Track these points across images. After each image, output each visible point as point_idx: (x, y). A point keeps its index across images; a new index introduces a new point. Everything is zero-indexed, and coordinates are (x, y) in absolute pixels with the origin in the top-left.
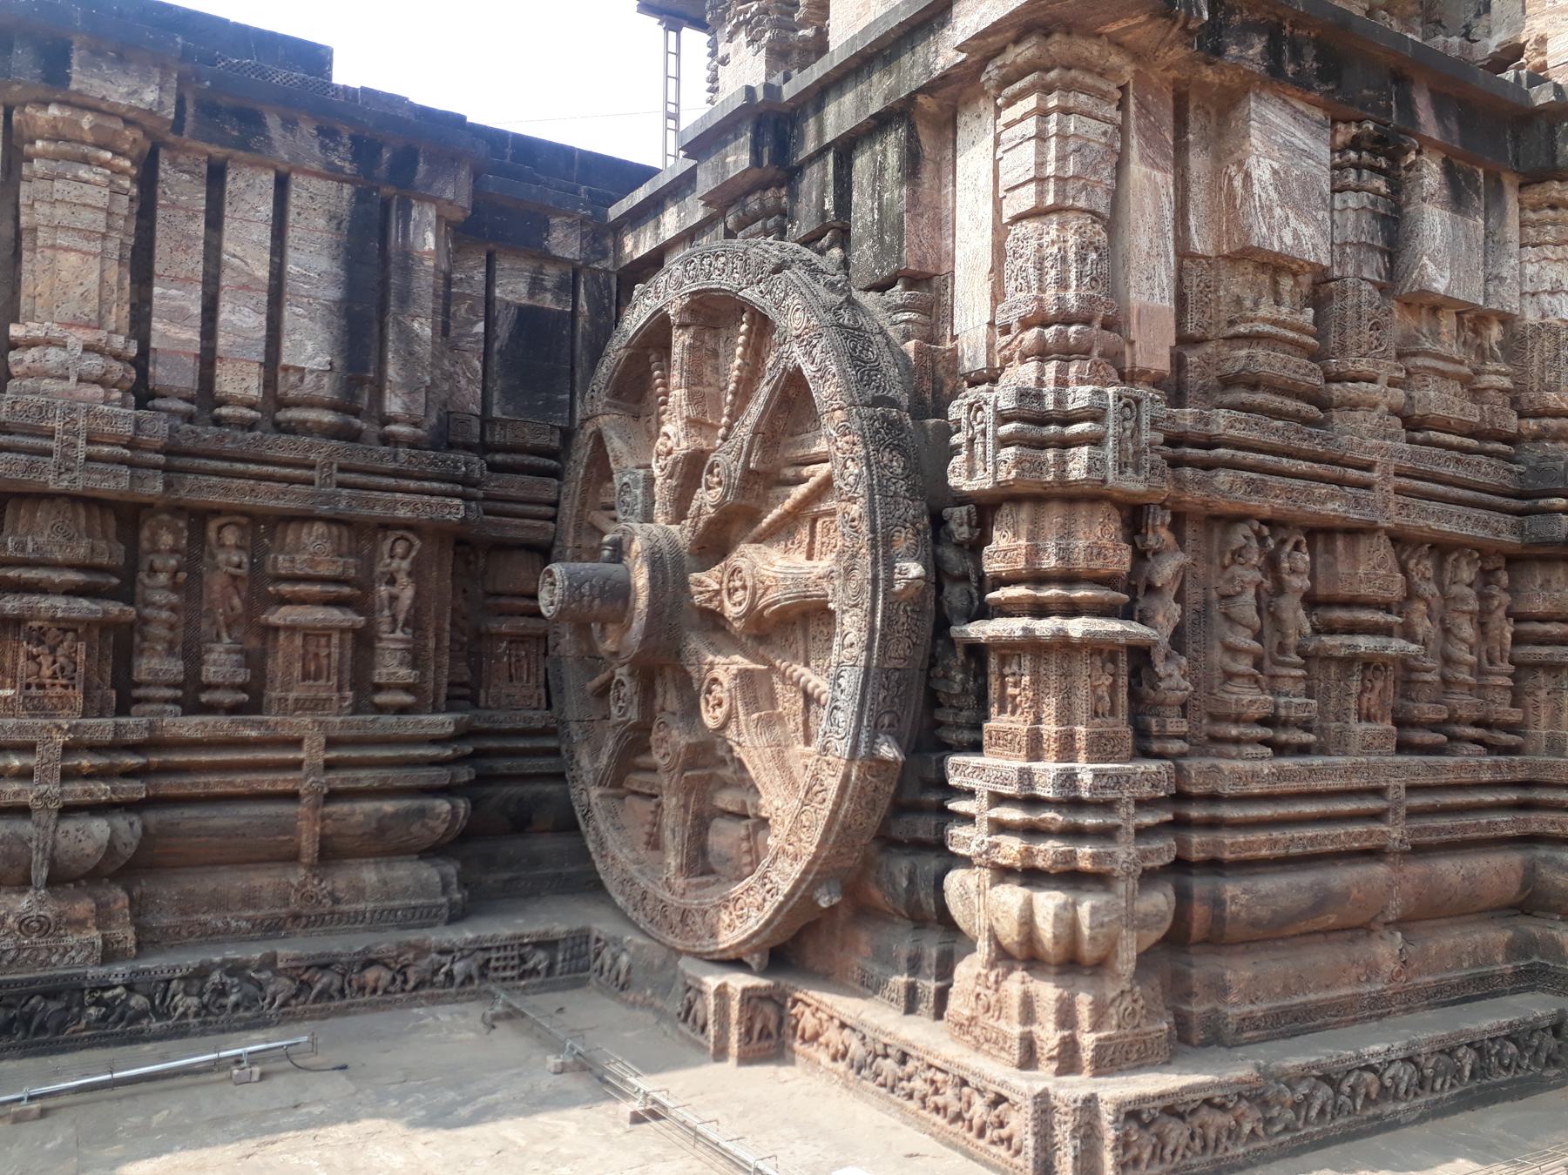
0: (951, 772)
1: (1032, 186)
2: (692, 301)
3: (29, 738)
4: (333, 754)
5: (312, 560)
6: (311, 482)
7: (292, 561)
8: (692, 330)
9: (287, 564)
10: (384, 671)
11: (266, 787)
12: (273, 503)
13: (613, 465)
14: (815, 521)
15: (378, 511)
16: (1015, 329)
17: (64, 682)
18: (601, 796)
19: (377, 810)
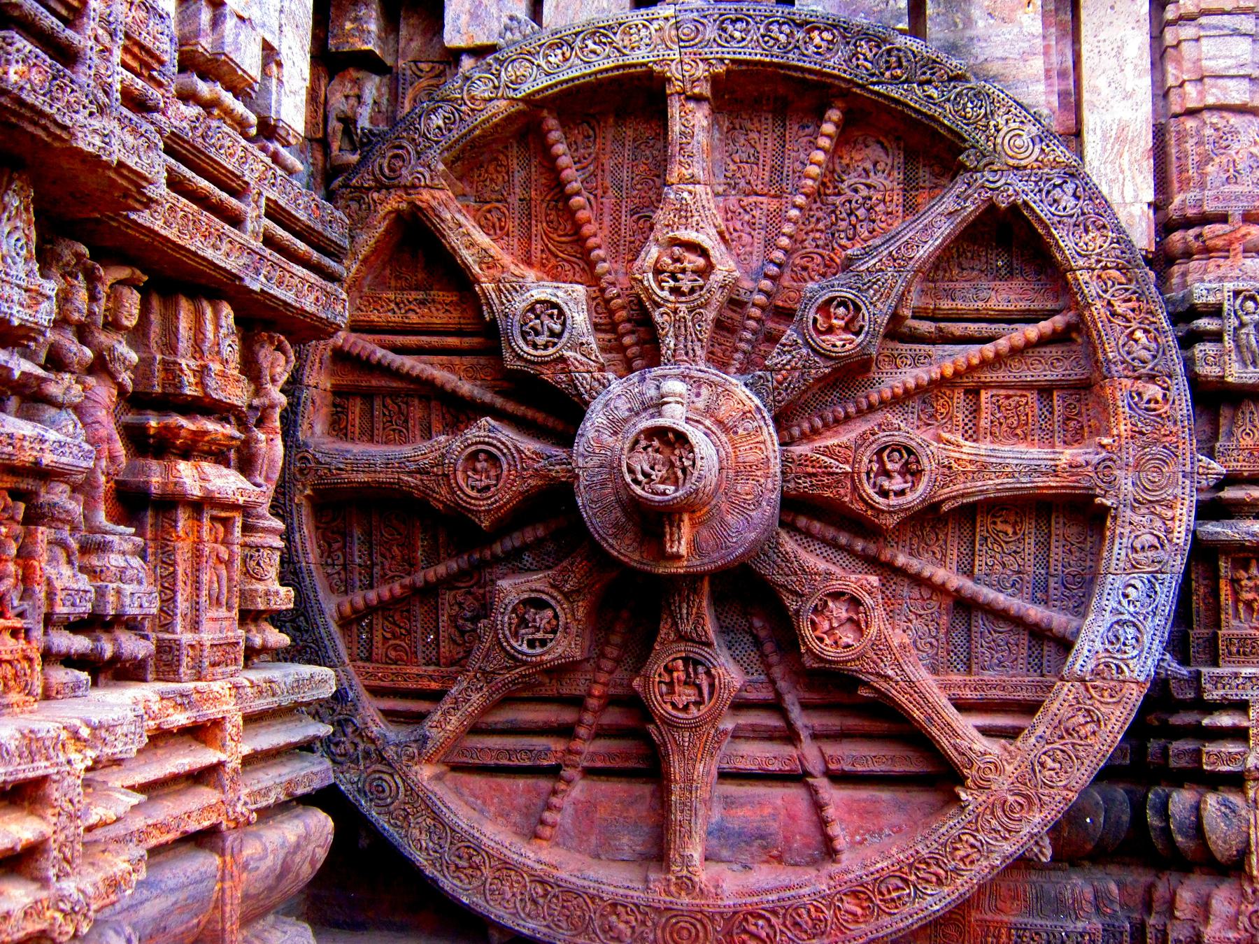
0: (1208, 686)
1: (1245, 84)
2: (728, 71)
3: (41, 767)
4: (246, 749)
5: (223, 375)
6: (236, 221)
7: (203, 372)
8: (706, 108)
9: (192, 380)
10: (260, 587)
11: (193, 826)
12: (209, 254)
13: (476, 269)
14: (974, 392)
15: (288, 296)
16: (1236, 217)
17: (18, 623)
18: (430, 779)
19: (283, 846)
